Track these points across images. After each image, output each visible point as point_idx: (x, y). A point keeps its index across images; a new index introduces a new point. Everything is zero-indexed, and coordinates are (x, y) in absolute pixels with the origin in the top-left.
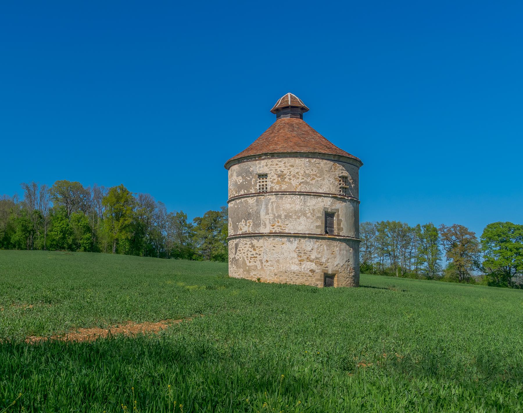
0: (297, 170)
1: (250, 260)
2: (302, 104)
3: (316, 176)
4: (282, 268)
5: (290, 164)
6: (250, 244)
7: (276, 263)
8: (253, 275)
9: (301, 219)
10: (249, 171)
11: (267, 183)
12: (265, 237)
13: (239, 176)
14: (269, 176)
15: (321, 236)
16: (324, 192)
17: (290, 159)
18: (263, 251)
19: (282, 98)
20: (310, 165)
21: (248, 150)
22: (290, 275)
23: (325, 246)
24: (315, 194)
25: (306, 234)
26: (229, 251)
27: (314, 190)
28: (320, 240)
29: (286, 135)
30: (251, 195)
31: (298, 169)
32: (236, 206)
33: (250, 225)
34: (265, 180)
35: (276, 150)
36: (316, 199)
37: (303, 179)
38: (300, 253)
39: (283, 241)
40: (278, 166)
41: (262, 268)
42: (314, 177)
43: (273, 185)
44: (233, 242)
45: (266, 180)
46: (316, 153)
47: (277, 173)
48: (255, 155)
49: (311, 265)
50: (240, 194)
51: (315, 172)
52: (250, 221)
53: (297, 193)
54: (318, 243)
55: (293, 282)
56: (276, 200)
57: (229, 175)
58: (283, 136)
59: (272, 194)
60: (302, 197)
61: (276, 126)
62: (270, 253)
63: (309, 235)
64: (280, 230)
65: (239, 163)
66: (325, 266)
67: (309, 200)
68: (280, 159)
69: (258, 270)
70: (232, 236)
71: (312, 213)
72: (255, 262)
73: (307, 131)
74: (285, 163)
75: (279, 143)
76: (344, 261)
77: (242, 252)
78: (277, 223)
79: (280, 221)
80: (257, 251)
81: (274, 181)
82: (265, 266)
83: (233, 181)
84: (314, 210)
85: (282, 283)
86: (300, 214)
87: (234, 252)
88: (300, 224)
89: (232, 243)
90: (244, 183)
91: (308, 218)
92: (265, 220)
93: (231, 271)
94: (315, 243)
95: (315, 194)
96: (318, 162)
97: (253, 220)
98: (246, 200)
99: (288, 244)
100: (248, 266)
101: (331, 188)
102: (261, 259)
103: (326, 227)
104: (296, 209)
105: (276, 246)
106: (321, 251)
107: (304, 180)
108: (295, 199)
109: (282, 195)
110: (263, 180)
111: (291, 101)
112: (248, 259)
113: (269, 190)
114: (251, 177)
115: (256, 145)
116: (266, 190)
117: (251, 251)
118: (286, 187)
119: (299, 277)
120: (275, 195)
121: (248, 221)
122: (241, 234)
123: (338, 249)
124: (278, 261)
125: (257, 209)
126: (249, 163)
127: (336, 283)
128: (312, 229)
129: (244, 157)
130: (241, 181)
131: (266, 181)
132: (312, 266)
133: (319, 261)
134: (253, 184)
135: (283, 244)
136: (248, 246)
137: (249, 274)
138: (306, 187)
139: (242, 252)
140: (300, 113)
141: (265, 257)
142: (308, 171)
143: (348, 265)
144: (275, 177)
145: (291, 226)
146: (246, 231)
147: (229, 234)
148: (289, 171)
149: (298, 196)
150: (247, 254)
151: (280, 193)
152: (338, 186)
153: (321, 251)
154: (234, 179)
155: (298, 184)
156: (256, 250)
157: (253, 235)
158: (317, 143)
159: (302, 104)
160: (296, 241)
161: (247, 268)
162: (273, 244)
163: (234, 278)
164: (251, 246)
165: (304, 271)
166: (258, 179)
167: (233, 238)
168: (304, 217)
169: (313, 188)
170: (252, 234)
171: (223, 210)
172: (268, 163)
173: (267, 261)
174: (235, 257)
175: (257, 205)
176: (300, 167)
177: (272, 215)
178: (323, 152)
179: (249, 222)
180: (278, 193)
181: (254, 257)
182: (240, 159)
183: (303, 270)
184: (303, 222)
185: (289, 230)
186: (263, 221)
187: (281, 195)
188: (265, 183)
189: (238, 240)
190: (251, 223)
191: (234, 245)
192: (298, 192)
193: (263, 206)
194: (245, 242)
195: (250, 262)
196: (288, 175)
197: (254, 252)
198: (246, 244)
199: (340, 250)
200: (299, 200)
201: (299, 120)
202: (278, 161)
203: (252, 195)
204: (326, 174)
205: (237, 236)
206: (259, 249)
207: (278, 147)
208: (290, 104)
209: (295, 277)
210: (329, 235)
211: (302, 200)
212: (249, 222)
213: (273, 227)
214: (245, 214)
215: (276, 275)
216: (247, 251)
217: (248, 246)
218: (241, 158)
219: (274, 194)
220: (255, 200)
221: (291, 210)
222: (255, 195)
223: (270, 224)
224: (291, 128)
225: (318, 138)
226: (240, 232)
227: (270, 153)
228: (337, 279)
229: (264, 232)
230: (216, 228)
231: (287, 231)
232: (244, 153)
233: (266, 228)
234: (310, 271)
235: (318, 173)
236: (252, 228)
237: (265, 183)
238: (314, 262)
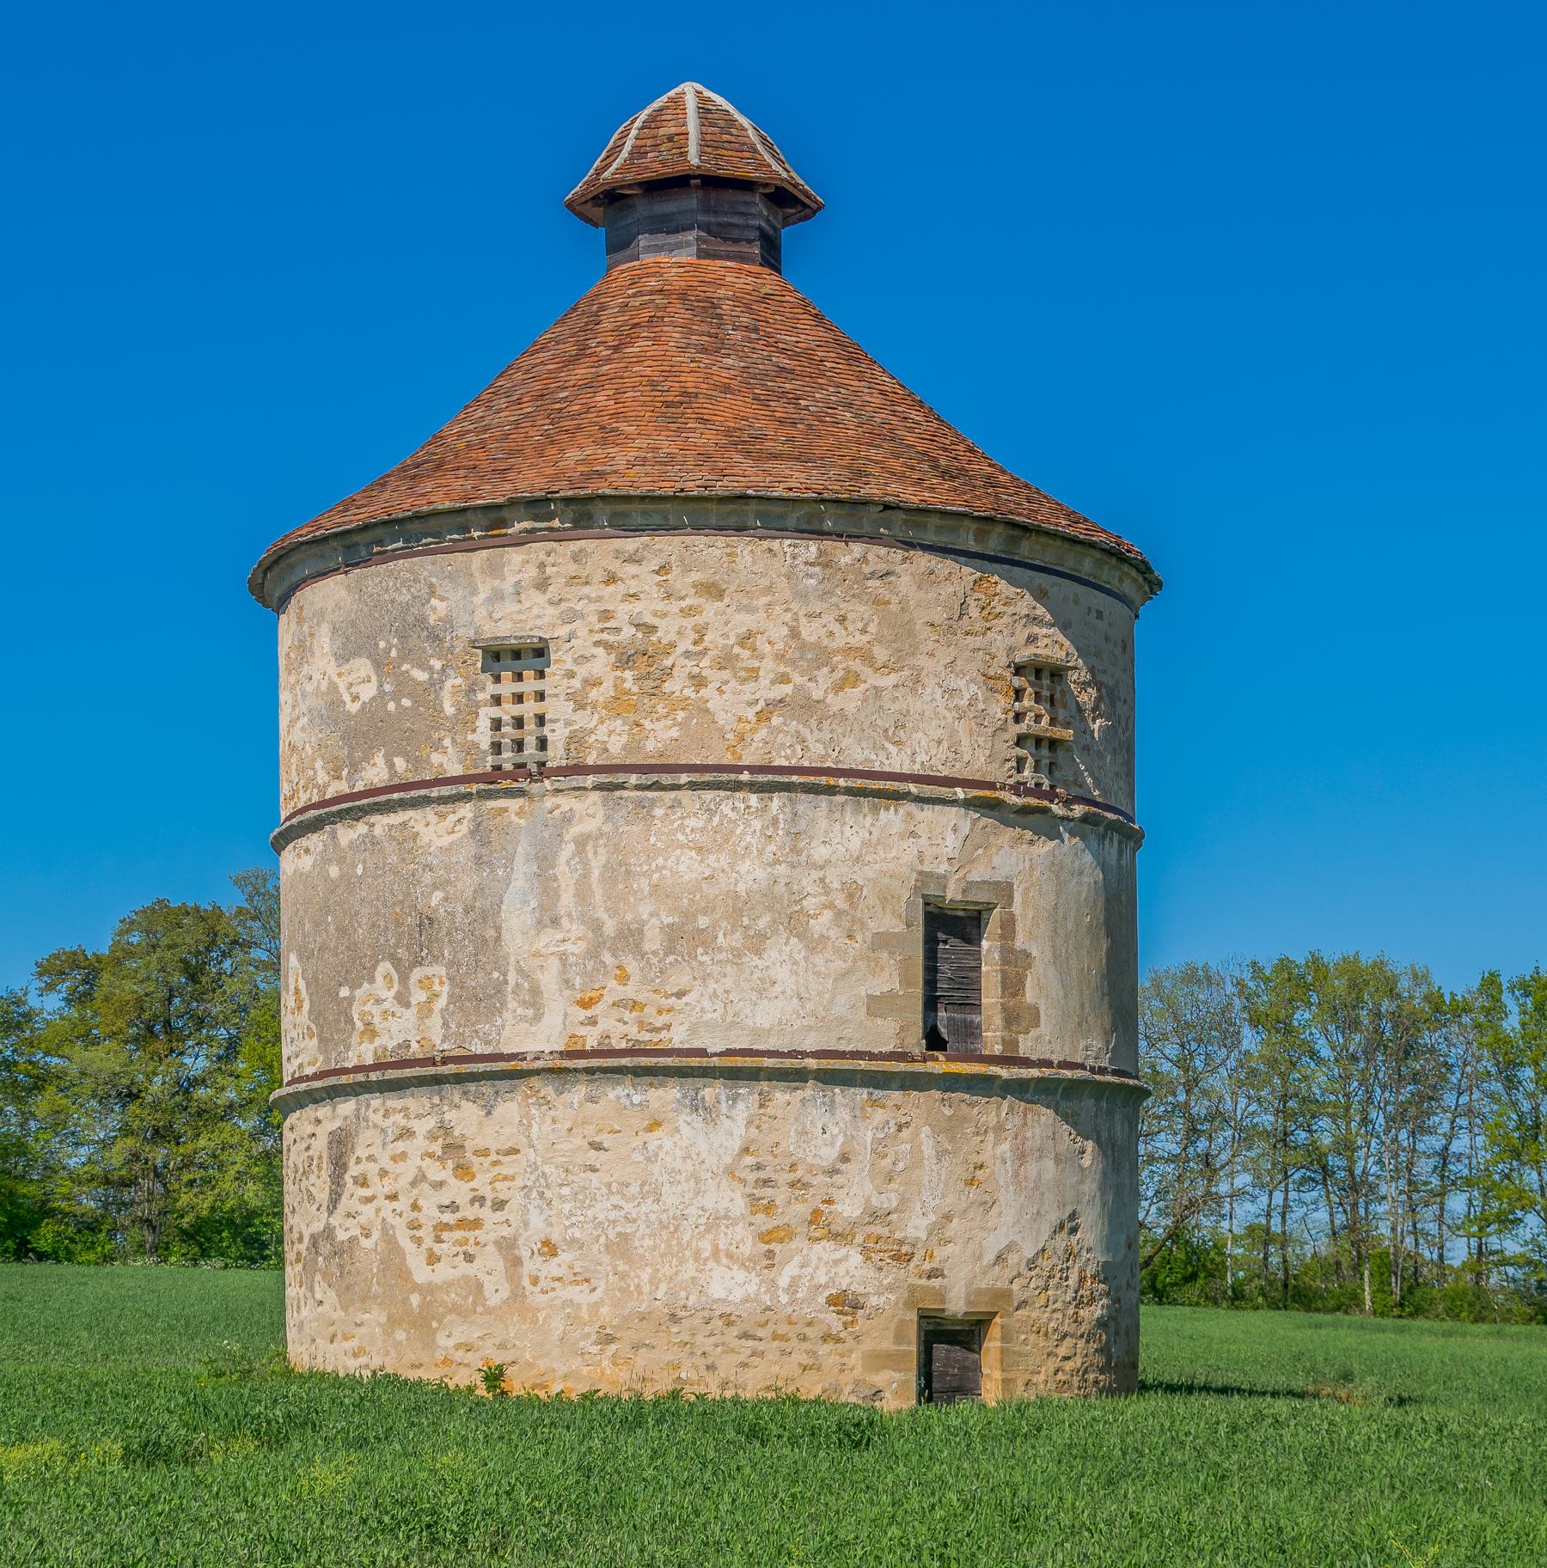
1: (437, 1247)
2: (775, 166)
3: (868, 658)
4: (646, 1289)
5: (696, 576)
6: (432, 1137)
7: (606, 1259)
8: (458, 1347)
9: (772, 954)
10: (421, 621)
11: (550, 708)
12: (535, 1081)
13: (356, 654)
14: (560, 660)
15: (902, 1067)
16: (917, 769)
17: (700, 541)
18: (519, 1182)
19: (643, 116)
20: (827, 586)
21: (413, 473)
22: (699, 1339)
23: (926, 1130)
24: (859, 783)
25: (804, 1055)
26: (289, 1186)
27: (857, 755)
28: (896, 1096)
29: (668, 374)
30: (435, 792)
31: (756, 610)
32: (334, 871)
33: (430, 1001)
34: (530, 685)
35: (601, 475)
36: (869, 820)
37: (784, 679)
38: (766, 1182)
39: (654, 1104)
40: (620, 588)
41: (517, 1295)
42: (857, 665)
43: (584, 720)
44: (318, 1121)
45: (539, 685)
46: (865, 503)
47: (611, 638)
48: (464, 510)
49: (837, 1262)
50: (359, 787)
51: (864, 631)
52: (429, 971)
53: (745, 777)
54: (879, 1116)
55: (724, 1385)
56: (607, 828)
57: (282, 650)
58: (653, 385)
59: (577, 781)
60: (777, 801)
61: (603, 308)
62: (566, 1191)
63: (826, 1064)
64: (633, 1031)
65: (356, 565)
66: (927, 1266)
67: (823, 824)
68: (631, 544)
69: (489, 1311)
70: (308, 1078)
71: (839, 914)
72: (469, 1258)
73: (808, 354)
74: (663, 569)
75: (623, 426)
76: (1046, 1229)
77: (378, 1188)
78: (612, 984)
79: (632, 967)
80: (481, 1183)
81: (594, 694)
82: (535, 1281)
83: (309, 687)
84: (852, 893)
85: (648, 1396)
86: (763, 923)
87: (323, 1196)
88: (765, 987)
89: (309, 1129)
90: (391, 706)
91: (814, 945)
92: (536, 962)
93: (300, 1326)
94: (860, 1116)
95: (859, 783)
96: (882, 567)
97: (450, 964)
98: (404, 824)
99: (688, 1126)
100: (416, 1288)
101: (965, 742)
102: (505, 1231)
103: (931, 1004)
104: (741, 888)
105: (606, 1139)
106: (901, 1166)
107: (787, 689)
108: (733, 815)
109: (648, 788)
110: (518, 687)
111: (704, 144)
112: (418, 1241)
113: (561, 752)
114: (437, 664)
115: (471, 437)
116: (540, 756)
117: (438, 1185)
118: (674, 733)
119: (761, 1346)
120: (598, 787)
121: (417, 974)
122: (378, 1066)
123: (1005, 1147)
124: (621, 1247)
125: (480, 890)
126: (426, 567)
127: (998, 1375)
128: (842, 1021)
129: (384, 523)
130: (368, 692)
131: (541, 696)
132: (841, 1269)
133: (885, 1232)
134: (449, 710)
135: (655, 1125)
136: (419, 1143)
137: (431, 1345)
138: (806, 732)
139: (378, 1188)
140: (759, 228)
141: (536, 1221)
142: (816, 623)
143: (1070, 1254)
144: (601, 663)
145: (706, 1004)
146: (406, 1045)
147: (289, 1070)
148: (689, 623)
149: (753, 799)
150: (415, 1207)
151: (633, 779)
152: (1003, 729)
153: (901, 1166)
154: (317, 676)
155: (750, 714)
156: (473, 1177)
157: (451, 1068)
158: (874, 436)
159: (775, 166)
160: (741, 1105)
161: (415, 1299)
162: (590, 1130)
163: (323, 1376)
164: (437, 1147)
165: (791, 1303)
166: (487, 678)
167: (313, 1098)
168: (794, 940)
169: (846, 742)
170: (445, 1061)
171: (250, 899)
172: (549, 570)
173: (549, 1249)
174: (329, 1232)
175: (478, 860)
176: (764, 600)
177: (577, 929)
178: (910, 495)
179: (426, 983)
180: (620, 778)
181: (462, 1224)
182: (356, 538)
183: (784, 1299)
184: (782, 974)
185: (693, 1030)
186: (520, 971)
187: (638, 787)
188: (529, 709)
189: (347, 1107)
190: (437, 987)
191: (320, 1145)
192: (753, 769)
193: (523, 868)
194: (398, 1118)
195: (433, 1259)
196: (687, 654)
197: (459, 1191)
198: (406, 1133)
199: (1021, 1157)
200: (757, 824)
201: (758, 275)
202: (618, 554)
203: (446, 791)
204: (931, 645)
205: (344, 1079)
206: (495, 1163)
207: (622, 458)
208: (695, 161)
209: (732, 1351)
210: (949, 1059)
211: (775, 821)
212: (426, 983)
213: (589, 1013)
214: (398, 924)
215: (609, 1339)
216: (413, 1184)
217: (419, 1143)
218: (366, 528)
219: (590, 780)
220: (464, 828)
221: (710, 890)
222: (463, 789)
223: (567, 993)
224: (705, 328)
225: (877, 400)
226: (363, 1052)
227: (568, 501)
228: (1003, 1351)
229: (530, 1047)
230: (200, 1022)
231: (678, 1037)
232: (386, 495)
233: (538, 1018)
234: (833, 1301)
235: (879, 639)
236: (446, 1024)
237: (529, 709)
238: (859, 1239)
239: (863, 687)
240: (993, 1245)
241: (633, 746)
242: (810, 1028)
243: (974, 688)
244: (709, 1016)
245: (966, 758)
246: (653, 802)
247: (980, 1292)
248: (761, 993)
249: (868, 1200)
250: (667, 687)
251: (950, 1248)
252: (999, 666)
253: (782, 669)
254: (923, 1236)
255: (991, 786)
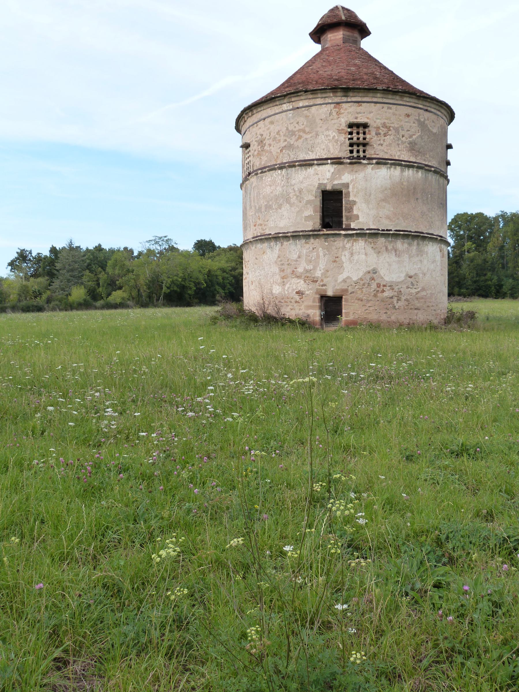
0: (277, 128)
3: (304, 131)
9: (283, 209)
16: (318, 157)
23: (321, 249)
24: (301, 163)
37: (285, 140)
42: (301, 134)
49: (298, 283)
51: (303, 125)
54: (307, 246)
63: (295, 234)
66: (322, 283)
67: (294, 175)
71: (297, 196)
84: (300, 191)
91: (292, 205)
106: (313, 258)
107: (286, 143)
108: (275, 176)
132: (299, 285)
138: (290, 153)
142: (292, 125)
145: (271, 223)
149: (279, 171)
153: (313, 258)
155: (279, 151)
160: (278, 246)
168: (287, 204)
184: (285, 213)
200: (280, 177)
204: (320, 125)
211: (283, 176)
234: (297, 293)
238: (303, 277)
239: (302, 139)
240: (341, 278)
241: (260, 164)
242: (291, 226)
243: (334, 134)
244: (272, 225)
245: (332, 152)
246: (263, 176)
247: (337, 289)
248: (281, 218)
249: (305, 268)
250: (265, 148)
251: (328, 279)
252: (344, 126)
253: (285, 138)
254: (320, 275)
255: (340, 158)
